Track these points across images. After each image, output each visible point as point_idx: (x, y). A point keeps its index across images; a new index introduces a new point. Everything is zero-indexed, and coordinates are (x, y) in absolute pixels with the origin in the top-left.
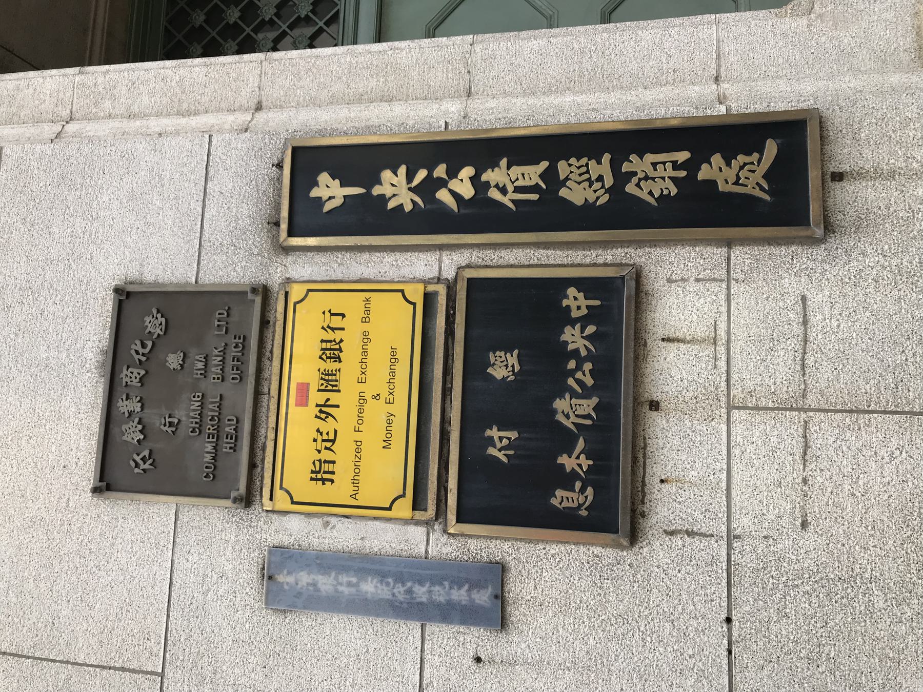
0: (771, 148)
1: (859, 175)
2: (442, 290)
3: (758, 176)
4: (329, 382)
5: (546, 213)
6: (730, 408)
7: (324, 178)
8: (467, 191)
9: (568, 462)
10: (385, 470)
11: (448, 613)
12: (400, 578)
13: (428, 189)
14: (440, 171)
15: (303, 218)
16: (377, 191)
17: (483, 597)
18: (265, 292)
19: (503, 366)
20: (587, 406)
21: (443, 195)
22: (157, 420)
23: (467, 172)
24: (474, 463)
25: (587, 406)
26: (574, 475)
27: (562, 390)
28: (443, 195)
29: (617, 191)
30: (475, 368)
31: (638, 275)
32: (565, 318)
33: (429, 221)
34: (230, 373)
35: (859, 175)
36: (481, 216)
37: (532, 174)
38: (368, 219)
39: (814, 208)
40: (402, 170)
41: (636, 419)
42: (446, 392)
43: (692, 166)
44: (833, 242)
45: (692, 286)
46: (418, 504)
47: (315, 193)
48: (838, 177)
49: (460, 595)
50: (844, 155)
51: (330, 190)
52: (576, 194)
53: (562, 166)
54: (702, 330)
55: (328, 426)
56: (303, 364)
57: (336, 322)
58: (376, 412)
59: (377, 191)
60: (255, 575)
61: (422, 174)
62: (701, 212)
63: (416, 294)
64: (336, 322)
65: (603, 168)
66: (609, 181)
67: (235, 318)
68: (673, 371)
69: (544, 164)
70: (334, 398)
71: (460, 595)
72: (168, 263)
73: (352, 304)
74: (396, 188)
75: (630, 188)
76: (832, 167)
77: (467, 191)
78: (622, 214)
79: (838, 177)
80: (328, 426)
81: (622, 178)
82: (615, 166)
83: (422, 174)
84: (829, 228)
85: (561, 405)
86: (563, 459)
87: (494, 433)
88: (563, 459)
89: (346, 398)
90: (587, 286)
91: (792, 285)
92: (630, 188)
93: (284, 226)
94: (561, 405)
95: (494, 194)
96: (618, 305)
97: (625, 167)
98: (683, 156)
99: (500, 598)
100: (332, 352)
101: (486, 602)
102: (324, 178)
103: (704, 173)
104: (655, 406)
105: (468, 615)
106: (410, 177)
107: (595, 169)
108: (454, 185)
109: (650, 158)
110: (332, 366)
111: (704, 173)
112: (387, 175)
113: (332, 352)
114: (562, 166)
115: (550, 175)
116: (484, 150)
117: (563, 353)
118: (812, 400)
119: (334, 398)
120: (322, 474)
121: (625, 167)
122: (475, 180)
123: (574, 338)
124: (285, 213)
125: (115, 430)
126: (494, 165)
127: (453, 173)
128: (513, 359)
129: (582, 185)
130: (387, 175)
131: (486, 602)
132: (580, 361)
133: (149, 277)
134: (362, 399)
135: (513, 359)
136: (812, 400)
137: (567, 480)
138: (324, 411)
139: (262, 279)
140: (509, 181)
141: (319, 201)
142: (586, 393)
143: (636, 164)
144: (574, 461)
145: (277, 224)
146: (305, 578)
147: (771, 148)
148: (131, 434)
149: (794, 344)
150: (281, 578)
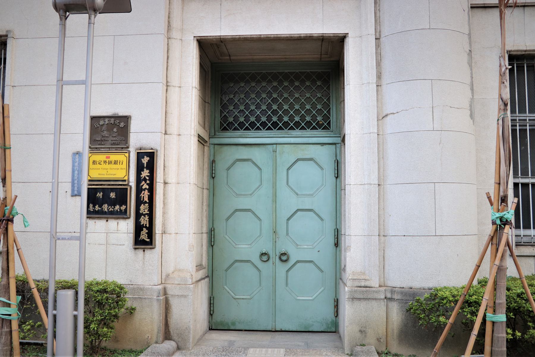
0: (148, 240)
1: (144, 254)
2: (126, 183)
3: (143, 238)
4: (110, 163)
5: (139, 202)
6: (107, 233)
7: (148, 158)
8: (143, 187)
9: (97, 207)
10: (95, 175)
11: (73, 186)
12: (78, 178)
13: (145, 180)
14: (148, 182)
15: (140, 156)
16: (145, 169)
17: (76, 192)
18: (128, 148)
19: (113, 195)
20: (106, 210)
21: (143, 182)
22: (104, 128)
23: (147, 187)
24: (96, 190)
25: (106, 210)
26: (95, 208)
27: (109, 205)
28: (143, 182)
29: (142, 214)
30: (112, 190)
31: (129, 218)
32: (121, 206)
33: (139, 180)
34: (112, 142)
35: (144, 254)
36: (139, 190)
37: (146, 199)
38: (140, 168)
39: (137, 247)
40: (149, 174)
41: (105, 218)
42: (109, 185)
43: (146, 227)
44: (133, 250)
45: (127, 227)
46: (90, 181)
47: (145, 157)
48: (144, 251)
49: (76, 189)
50: (148, 252)
51: (145, 160)
52: (142, 207)
53: (147, 205)
54: (119, 229)
55: (102, 163)
56: (114, 157)
57: (121, 163)
58: (105, 172)
59: (145, 169)
60: (78, 150)
61: (147, 178)
62: (138, 228)
63: (126, 178)
64: (121, 163)
65: (147, 212)
66: (144, 213)
67: (123, 142)
68: (113, 224)
69: (148, 201)
70: (107, 164)
71: (76, 189)
72: (134, 127)
73: (124, 166)
74: (145, 173)
75: (143, 217)
76: (146, 250)
77: (143, 187)
78: (138, 215)
79: (144, 251)
80: (102, 163)
81: (144, 215)
82: (147, 214)
83: (147, 178)
84: (135, 249)
85: (106, 205)
86: (97, 206)
87: (101, 194)
88: (97, 206)
89: (107, 166)
90: (126, 210)
91: (126, 243)
92: (143, 217)
93: (139, 151)
94: (106, 205)
95: (143, 192)
96: (123, 215)
97: (146, 216)
98: (148, 226)
99: (76, 195)
100: (116, 163)
101: (76, 194)
102: (148, 158)
103: (144, 229)
104: (107, 221)
105: (73, 190)
106: (147, 176)
107: (146, 210)
108: (145, 184)
109: (148, 220)
110: (113, 163)
111: (144, 229)
112: (148, 171)
113: (116, 163)
114: (147, 205)
115: (146, 202)
116: (151, 190)
117: (115, 205)
118: (108, 246)
119: (107, 164)
120: (94, 162)
121: (146, 216)
122: (146, 188)
123: (117, 207)
124: (141, 151)
125: (102, 119)
126: (148, 192)
127: (147, 184)
128: (114, 197)
129: (144, 209)
130: (148, 171)
131: (76, 194)
132: (113, 208)
133: (132, 122)
134: (107, 169)
135: (114, 197)
136: (108, 246)
137: (94, 206)
138: (105, 162)
139: (131, 146)
140: (145, 195)
141: (143, 158)
142: (108, 210)
143: (147, 217)
144: (97, 208)
145: (140, 149)
146: (77, 160)
147: (148, 240)
148: (101, 123)
149: (117, 243)
150: (77, 155)
